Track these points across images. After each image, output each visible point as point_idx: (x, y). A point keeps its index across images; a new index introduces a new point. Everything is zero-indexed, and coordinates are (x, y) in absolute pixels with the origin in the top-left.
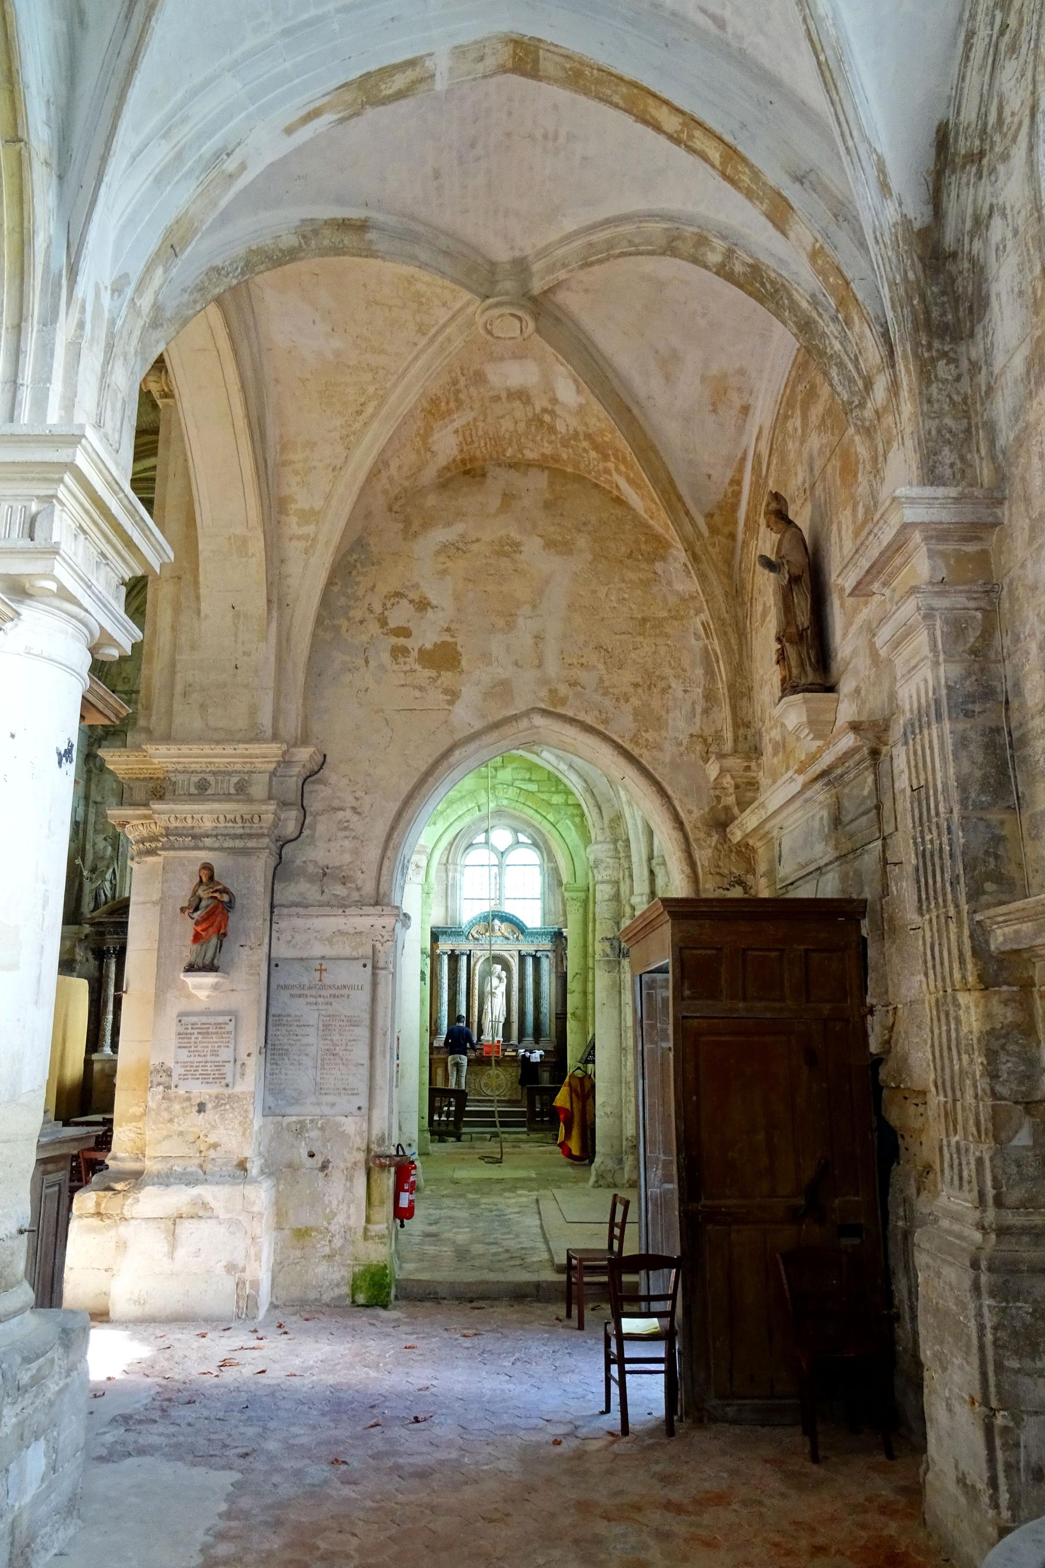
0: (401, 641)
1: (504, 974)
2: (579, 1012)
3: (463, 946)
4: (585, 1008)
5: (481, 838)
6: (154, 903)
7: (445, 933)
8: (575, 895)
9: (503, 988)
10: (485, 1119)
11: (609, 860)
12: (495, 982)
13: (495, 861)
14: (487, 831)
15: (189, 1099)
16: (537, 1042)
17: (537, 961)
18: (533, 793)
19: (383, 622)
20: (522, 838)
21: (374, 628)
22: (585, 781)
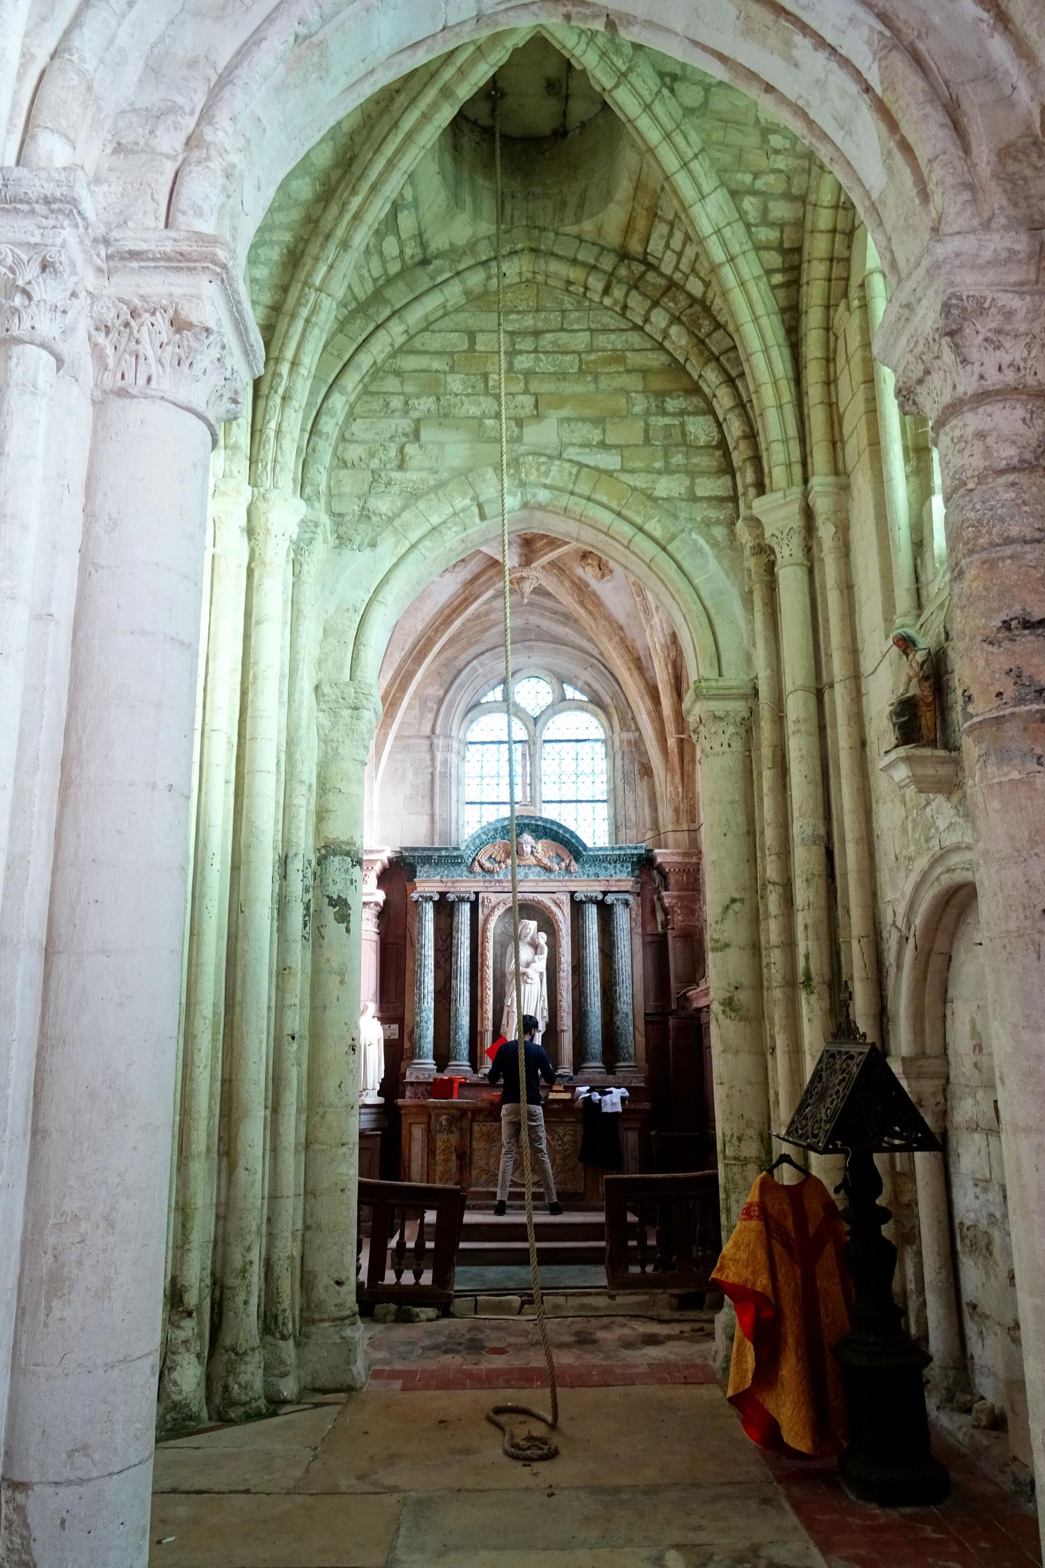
1: (542, 938)
2: (743, 997)
3: (464, 885)
4: (759, 986)
5: (497, 694)
7: (427, 860)
8: (719, 707)
9: (541, 964)
10: (507, 1247)
11: (1015, 303)
12: (526, 953)
13: (520, 732)
14: (504, 682)
16: (610, 1068)
17: (606, 912)
18: (609, 473)
20: (570, 692)
22: (883, 17)
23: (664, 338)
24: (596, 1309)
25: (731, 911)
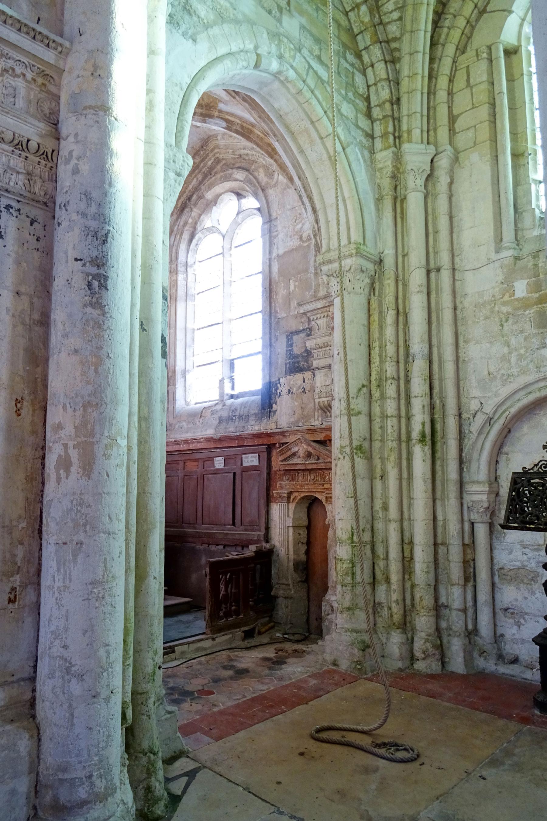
23: (353, 9)
24: (205, 649)
25: (362, 392)
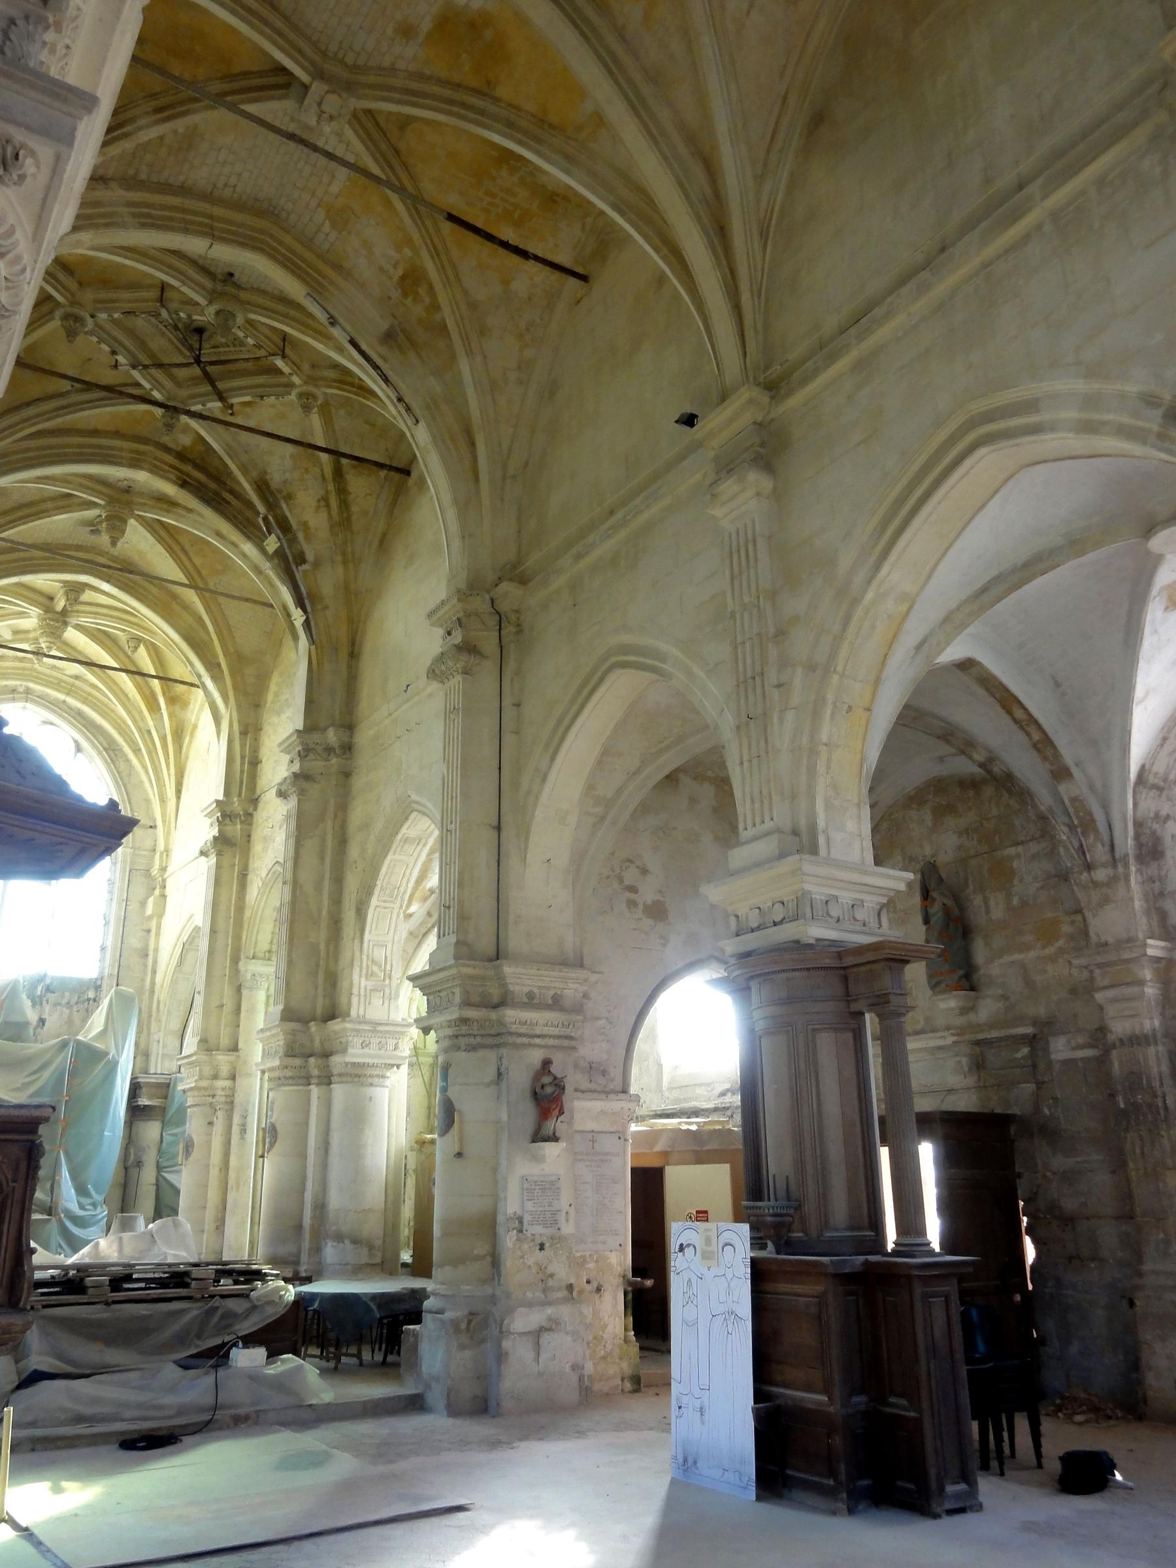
0: (632, 896)
6: (489, 1085)
15: (533, 1240)
19: (621, 880)
21: (616, 885)
